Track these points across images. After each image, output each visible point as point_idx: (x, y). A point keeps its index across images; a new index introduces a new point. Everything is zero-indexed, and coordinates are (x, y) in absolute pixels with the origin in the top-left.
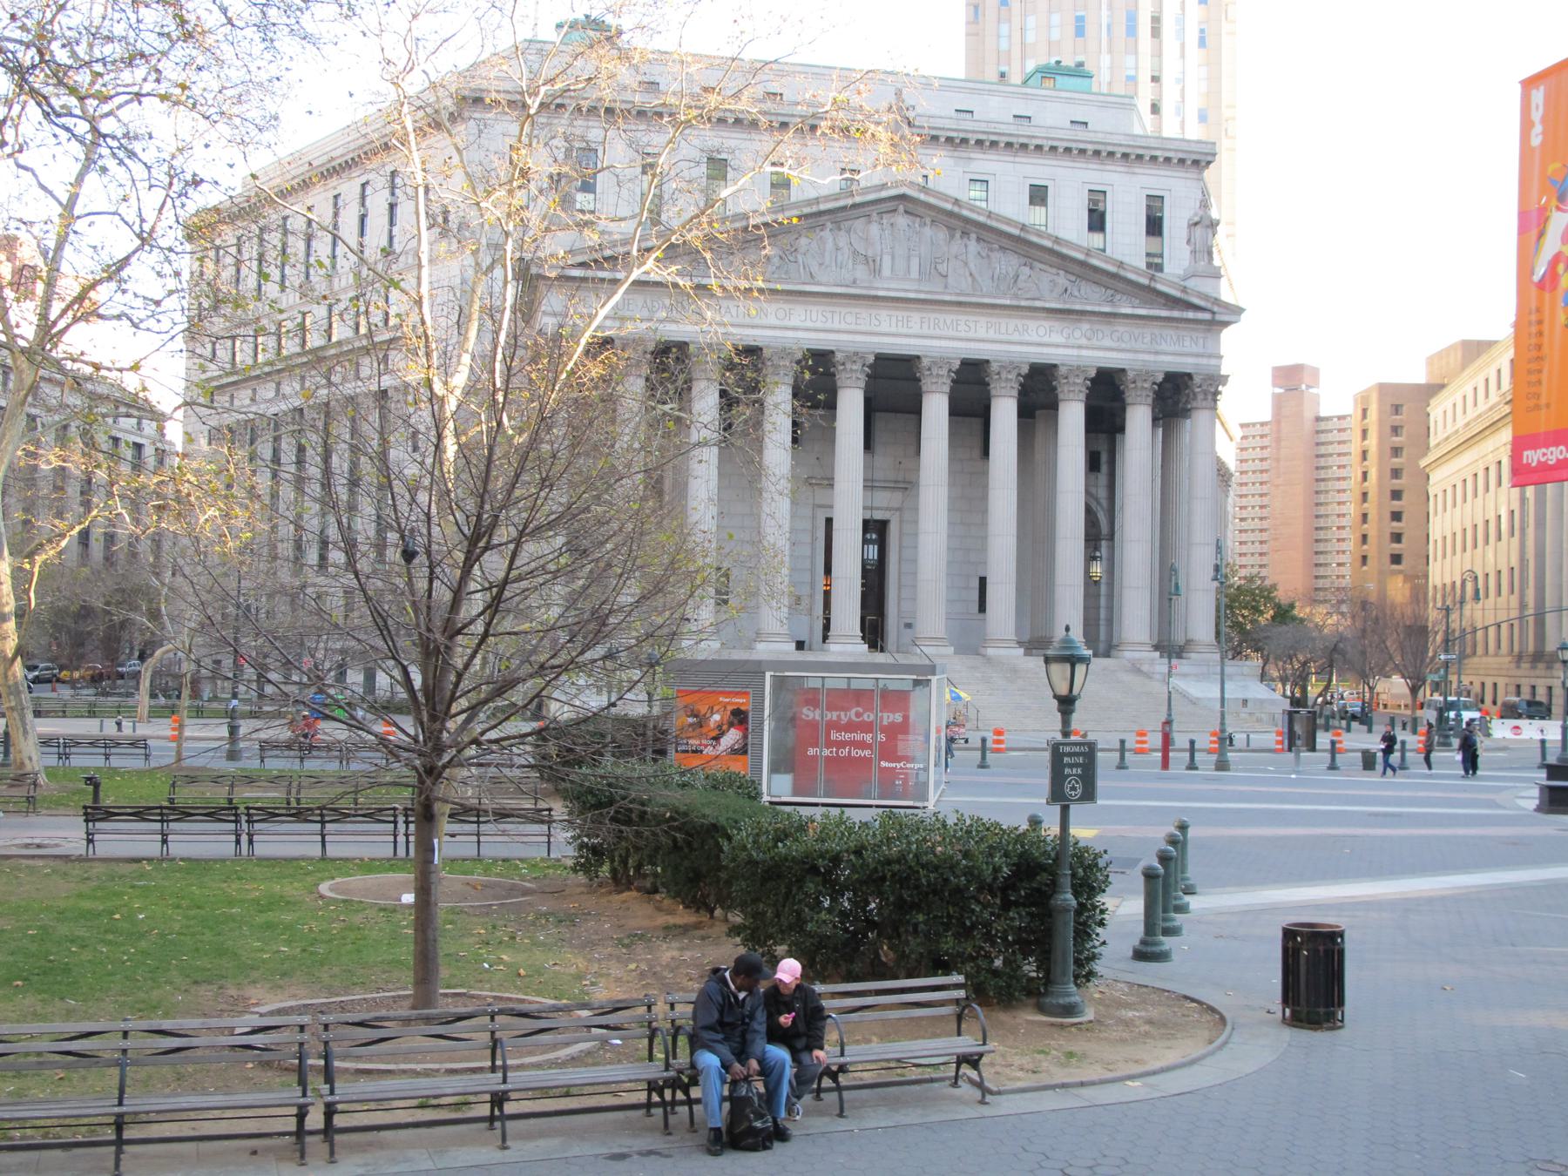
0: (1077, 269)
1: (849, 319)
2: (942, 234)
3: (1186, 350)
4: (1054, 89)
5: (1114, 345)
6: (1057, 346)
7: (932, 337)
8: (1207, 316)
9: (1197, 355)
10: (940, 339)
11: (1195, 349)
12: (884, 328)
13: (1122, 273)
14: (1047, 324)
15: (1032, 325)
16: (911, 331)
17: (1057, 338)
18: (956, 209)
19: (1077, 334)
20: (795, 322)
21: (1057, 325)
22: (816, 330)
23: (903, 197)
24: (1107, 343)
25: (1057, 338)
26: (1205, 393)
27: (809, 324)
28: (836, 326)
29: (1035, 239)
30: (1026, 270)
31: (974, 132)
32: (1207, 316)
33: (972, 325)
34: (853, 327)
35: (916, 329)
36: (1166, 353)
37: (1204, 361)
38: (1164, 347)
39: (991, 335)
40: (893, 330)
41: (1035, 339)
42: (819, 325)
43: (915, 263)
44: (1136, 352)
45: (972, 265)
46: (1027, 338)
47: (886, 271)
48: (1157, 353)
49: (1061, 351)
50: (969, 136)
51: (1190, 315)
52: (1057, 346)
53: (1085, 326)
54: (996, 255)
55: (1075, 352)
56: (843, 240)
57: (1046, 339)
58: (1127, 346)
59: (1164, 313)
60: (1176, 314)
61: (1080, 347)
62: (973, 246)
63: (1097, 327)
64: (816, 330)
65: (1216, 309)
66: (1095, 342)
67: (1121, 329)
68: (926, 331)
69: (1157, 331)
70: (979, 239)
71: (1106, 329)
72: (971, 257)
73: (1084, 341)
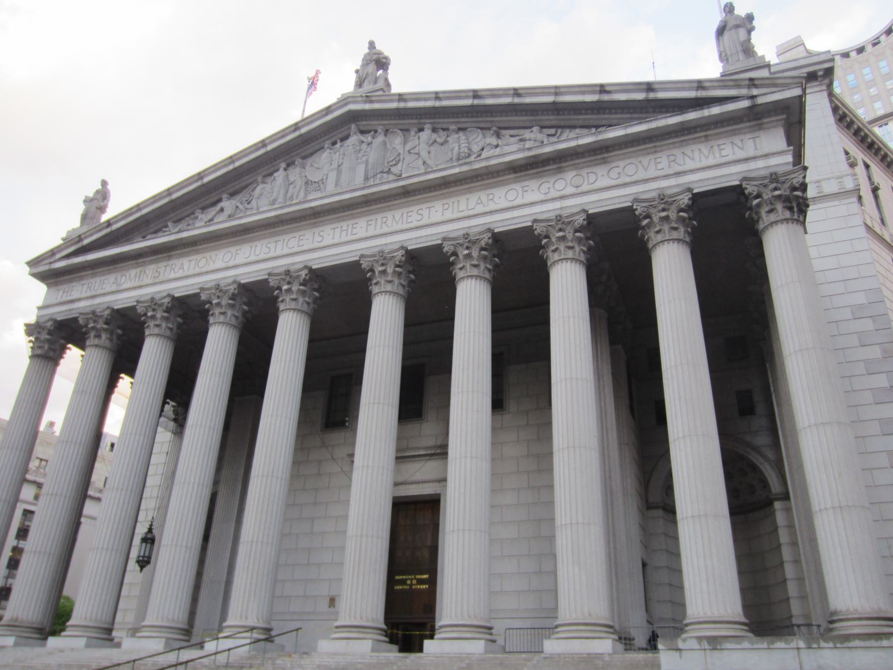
0: (552, 119)
2: (397, 141)
6: (532, 204)
9: (746, 160)
11: (741, 155)
12: (328, 241)
14: (517, 186)
19: (560, 185)
20: (240, 260)
28: (279, 252)
29: (490, 101)
30: (493, 141)
32: (745, 104)
35: (362, 233)
36: (692, 171)
37: (760, 164)
38: (690, 165)
39: (448, 215)
43: (361, 170)
45: (424, 154)
46: (492, 206)
48: (678, 174)
51: (716, 110)
52: (532, 204)
53: (570, 175)
55: (557, 205)
56: (295, 174)
58: (634, 178)
61: (562, 198)
63: (584, 172)
65: (755, 92)
67: (622, 164)
68: (371, 232)
71: (601, 170)
72: (423, 149)
73: (570, 190)
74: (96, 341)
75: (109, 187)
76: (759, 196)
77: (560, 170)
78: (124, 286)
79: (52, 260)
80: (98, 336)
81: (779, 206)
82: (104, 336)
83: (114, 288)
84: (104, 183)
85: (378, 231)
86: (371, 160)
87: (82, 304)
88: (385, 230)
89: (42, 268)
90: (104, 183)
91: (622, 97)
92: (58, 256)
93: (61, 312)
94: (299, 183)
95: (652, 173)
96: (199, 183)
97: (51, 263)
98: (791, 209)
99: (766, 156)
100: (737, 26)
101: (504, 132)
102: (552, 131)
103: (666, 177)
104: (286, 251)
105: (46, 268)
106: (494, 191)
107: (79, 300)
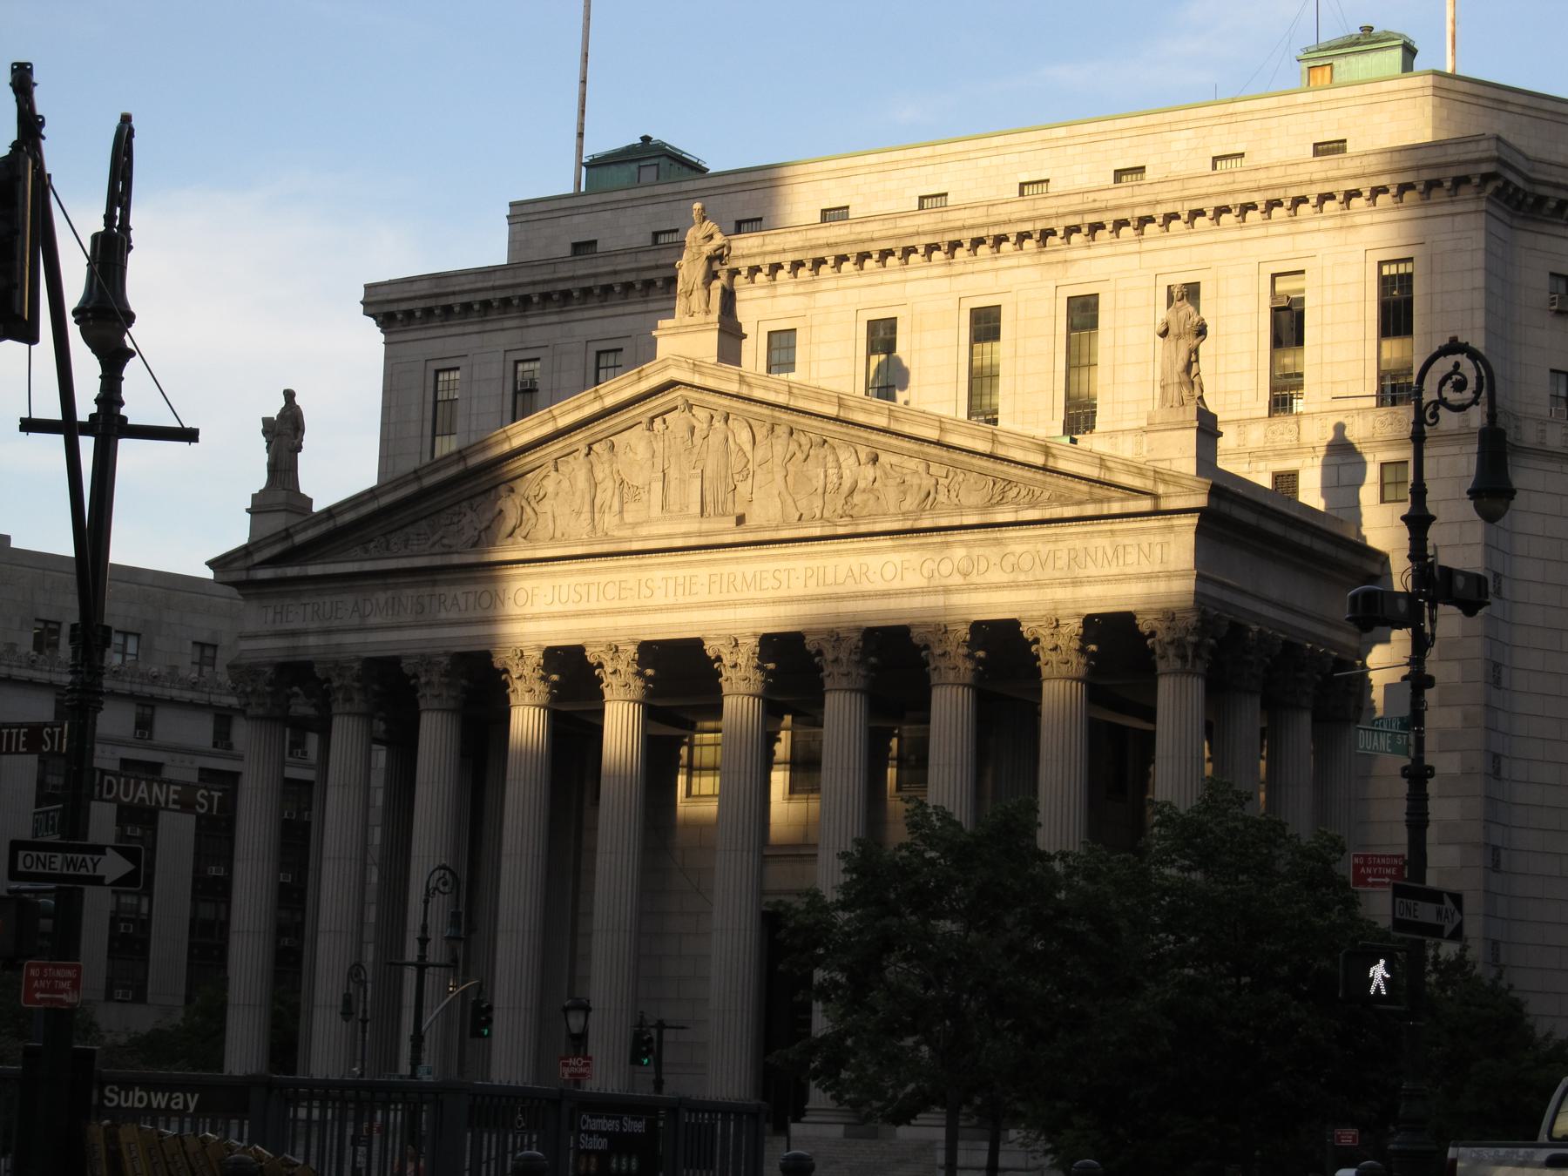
4: (1332, 85)
7: (687, 607)
16: (694, 599)
22: (564, 616)
31: (1057, 216)
32: (1145, 505)
33: (783, 576)
34: (616, 604)
48: (1076, 582)
50: (1052, 224)
62: (780, 446)
64: (564, 616)
65: (1161, 489)
74: (348, 707)
75: (298, 400)
78: (373, 620)
79: (249, 563)
80: (349, 700)
81: (1171, 652)
82: (357, 697)
83: (355, 621)
84: (289, 395)
86: (708, 473)
87: (312, 641)
90: (289, 395)
92: (258, 558)
96: (461, 467)
97: (248, 569)
98: (1183, 658)
105: (243, 576)
107: (306, 633)
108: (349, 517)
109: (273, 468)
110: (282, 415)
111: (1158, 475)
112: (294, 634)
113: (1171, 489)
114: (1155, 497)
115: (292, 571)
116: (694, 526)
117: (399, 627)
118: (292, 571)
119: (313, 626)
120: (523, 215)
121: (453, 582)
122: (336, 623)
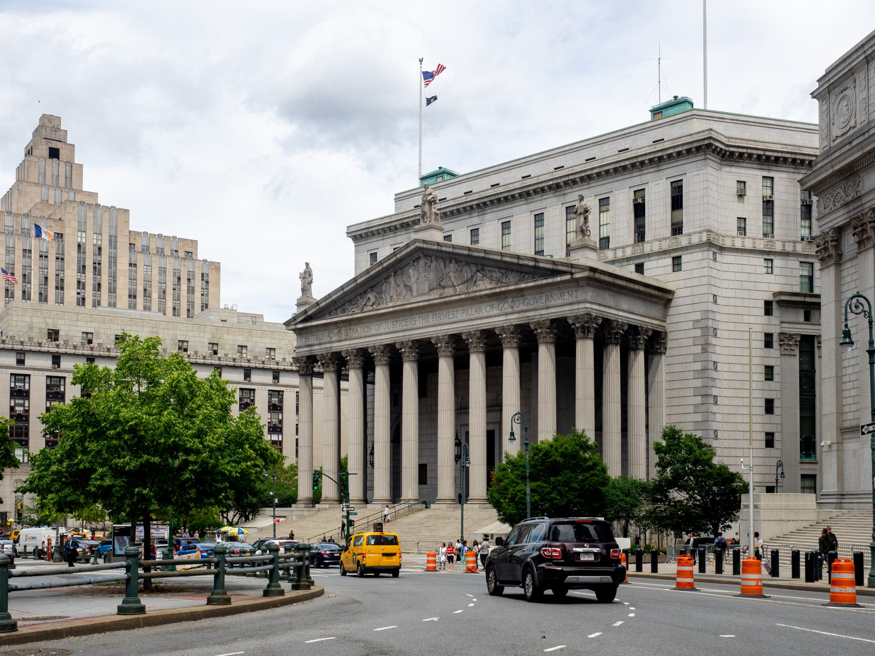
1: (403, 323)
3: (566, 301)
5: (525, 308)
8: (568, 277)
9: (571, 304)
10: (435, 327)
11: (571, 300)
12: (418, 325)
13: (521, 262)
15: (484, 306)
17: (496, 312)
18: (439, 248)
19: (506, 306)
20: (382, 330)
21: (495, 304)
23: (418, 249)
24: (522, 307)
25: (496, 312)
26: (577, 328)
27: (387, 330)
31: (561, 177)
32: (568, 277)
35: (431, 323)
37: (576, 307)
38: (553, 303)
39: (465, 317)
40: (421, 325)
41: (485, 314)
42: (391, 330)
44: (536, 310)
46: (481, 315)
47: (415, 294)
48: (548, 308)
49: (497, 319)
51: (559, 279)
52: (495, 316)
54: (465, 268)
57: (491, 313)
59: (544, 282)
60: (550, 280)
61: (506, 314)
64: (389, 333)
65: (573, 270)
66: (516, 309)
67: (529, 297)
69: (548, 294)
70: (457, 262)
73: (510, 310)
76: (574, 324)
77: (506, 298)
83: (329, 339)
84: (307, 264)
85: (437, 322)
87: (316, 347)
88: (440, 321)
89: (293, 327)
90: (307, 264)
91: (526, 262)
93: (305, 351)
94: (402, 286)
95: (539, 305)
98: (584, 332)
99: (578, 303)
100: (581, 214)
101: (486, 268)
102: (504, 271)
103: (544, 309)
104: (401, 328)
106: (481, 305)
107: (314, 345)
108: (323, 304)
109: (304, 290)
110: (305, 272)
111: (572, 266)
112: (311, 346)
113: (577, 270)
114: (572, 274)
115: (309, 324)
116: (426, 298)
117: (340, 341)
118: (309, 324)
119: (316, 342)
120: (399, 198)
121: (355, 325)
122: (323, 341)
